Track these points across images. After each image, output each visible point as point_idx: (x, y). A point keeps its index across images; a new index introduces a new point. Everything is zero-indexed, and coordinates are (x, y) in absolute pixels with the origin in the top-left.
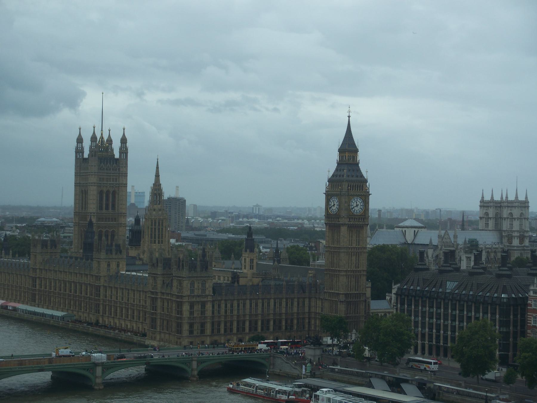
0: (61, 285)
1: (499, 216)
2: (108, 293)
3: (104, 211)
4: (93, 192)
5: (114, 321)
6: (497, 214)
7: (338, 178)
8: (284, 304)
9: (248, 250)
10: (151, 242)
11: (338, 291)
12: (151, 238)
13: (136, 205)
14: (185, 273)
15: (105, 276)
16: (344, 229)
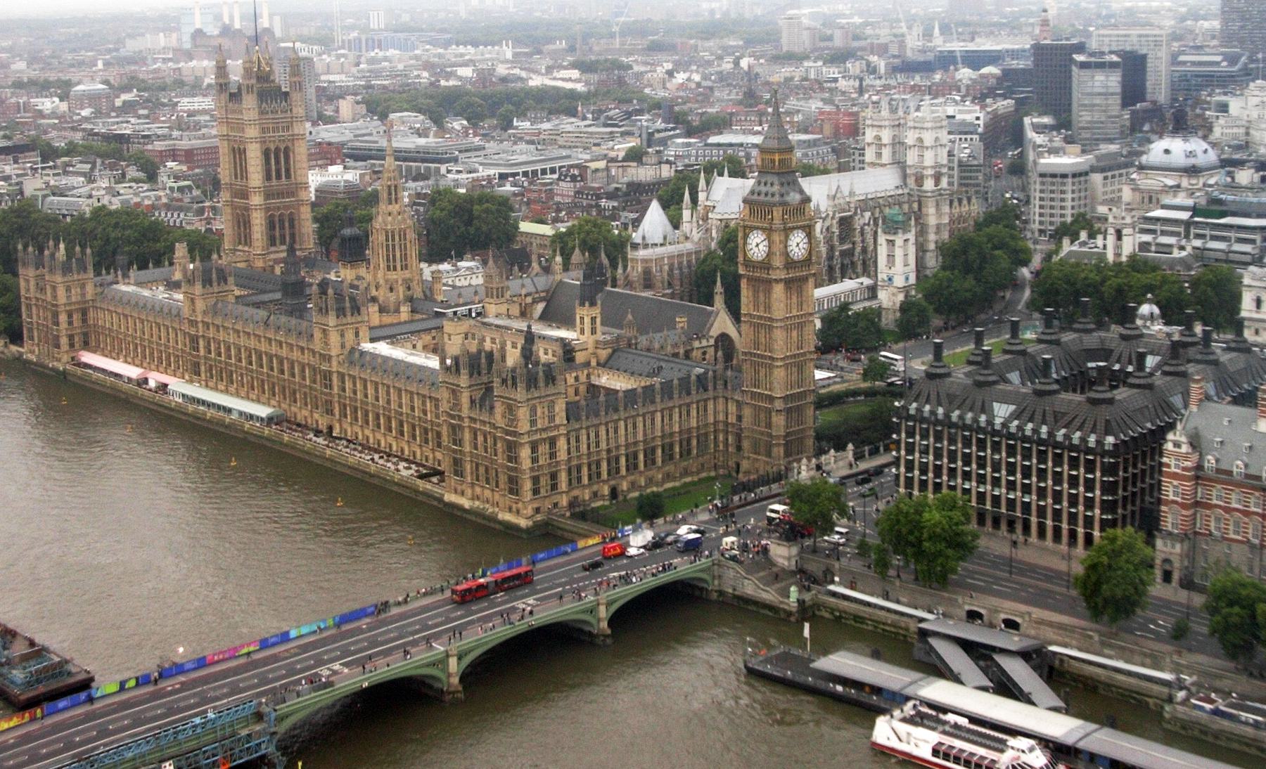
0: (250, 356)
1: (897, 141)
2: (348, 385)
3: (274, 182)
4: (254, 155)
5: (363, 431)
6: (894, 139)
7: (762, 198)
8: (676, 417)
9: (587, 304)
10: (389, 269)
11: (770, 390)
12: (388, 260)
13: (205, 30)
14: (520, 394)
15: (338, 356)
16: (778, 291)
